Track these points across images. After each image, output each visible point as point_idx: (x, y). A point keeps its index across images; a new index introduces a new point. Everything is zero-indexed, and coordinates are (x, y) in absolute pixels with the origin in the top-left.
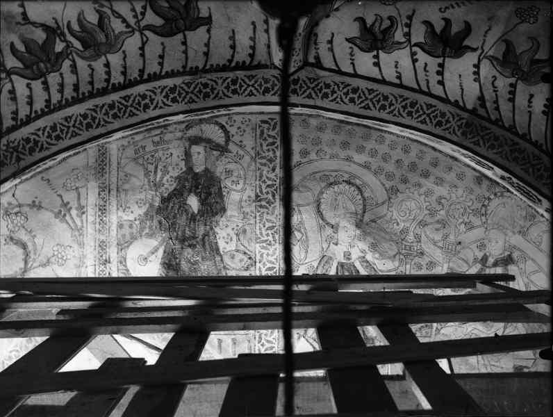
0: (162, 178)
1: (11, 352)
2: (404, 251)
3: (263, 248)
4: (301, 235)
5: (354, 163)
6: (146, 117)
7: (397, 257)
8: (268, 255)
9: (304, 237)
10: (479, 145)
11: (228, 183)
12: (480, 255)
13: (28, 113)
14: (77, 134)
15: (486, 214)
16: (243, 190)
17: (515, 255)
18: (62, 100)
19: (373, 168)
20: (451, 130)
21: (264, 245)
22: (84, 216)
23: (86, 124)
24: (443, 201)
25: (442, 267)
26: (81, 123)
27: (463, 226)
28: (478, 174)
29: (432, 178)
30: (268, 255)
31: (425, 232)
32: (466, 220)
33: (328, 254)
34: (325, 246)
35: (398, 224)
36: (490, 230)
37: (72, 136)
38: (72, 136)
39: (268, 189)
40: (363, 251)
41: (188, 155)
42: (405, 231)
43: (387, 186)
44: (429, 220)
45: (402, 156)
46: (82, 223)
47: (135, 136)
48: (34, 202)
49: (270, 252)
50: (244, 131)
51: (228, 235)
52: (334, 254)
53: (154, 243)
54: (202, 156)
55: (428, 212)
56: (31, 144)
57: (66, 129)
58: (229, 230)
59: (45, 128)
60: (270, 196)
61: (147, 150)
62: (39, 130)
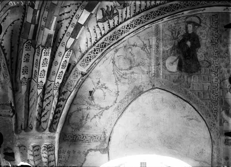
0: (178, 35)
1: (126, 96)
3: (214, 59)
4: (227, 54)
6: (178, 11)
8: (216, 62)
11: (201, 37)
13: (139, 11)
14: (154, 18)
16: (206, 39)
18: (140, 11)
21: (215, 58)
22: (151, 49)
23: (138, 23)
26: (156, 14)
30: (216, 62)
37: (153, 18)
38: (153, 18)
39: (216, 38)
41: (187, 28)
46: (150, 51)
47: (168, 21)
48: (134, 44)
49: (217, 61)
50: (206, 19)
51: (201, 55)
53: (175, 58)
54: (191, 28)
56: (139, 21)
57: (132, 25)
58: (202, 53)
59: (144, 16)
60: (216, 41)
61: (172, 26)
62: (142, 16)
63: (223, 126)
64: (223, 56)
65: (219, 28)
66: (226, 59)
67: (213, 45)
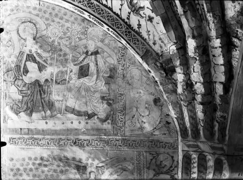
2: (53, 49)
4: (11, 43)
5: (32, 14)
7: (51, 51)
9: (13, 44)
12: (85, 51)
15: (87, 34)
17: (100, 50)
19: (40, 16)
24: (69, 29)
25: (70, 55)
27: (78, 38)
28: (83, 18)
29: (64, 20)
31: (62, 41)
32: (79, 36)
33: (23, 50)
34: (21, 47)
35: (51, 38)
36: (88, 40)
40: (37, 49)
42: (53, 41)
43: (46, 23)
44: (63, 36)
45: (52, 11)
52: (25, 51)
55: (63, 33)
64: (7, 45)
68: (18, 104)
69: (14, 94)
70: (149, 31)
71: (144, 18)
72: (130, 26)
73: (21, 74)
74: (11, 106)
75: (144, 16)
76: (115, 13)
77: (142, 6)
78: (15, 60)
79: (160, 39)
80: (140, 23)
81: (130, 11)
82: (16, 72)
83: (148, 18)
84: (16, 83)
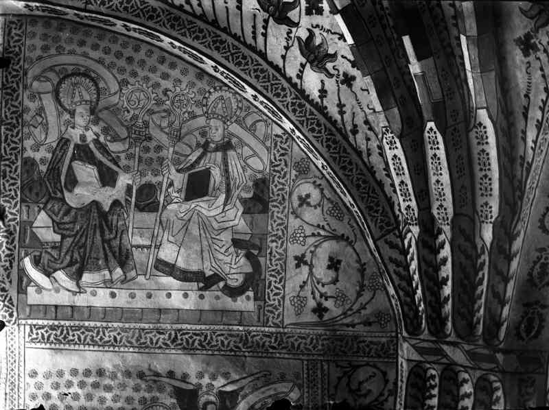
2: (133, 136)
3: (7, 129)
4: (41, 119)
5: (90, 58)
7: (128, 140)
8: (12, 136)
9: (45, 121)
10: (185, 35)
12: (202, 141)
15: (207, 105)
17: (234, 141)
19: (106, 64)
20: (161, 23)
24: (168, 93)
25: (168, 150)
27: (187, 114)
28: (199, 71)
29: (159, 74)
30: (12, 136)
31: (152, 119)
32: (189, 110)
33: (66, 136)
34: (63, 129)
35: (128, 112)
36: (210, 119)
40: (96, 134)
42: (135, 117)
43: (119, 79)
44: (156, 109)
45: (132, 54)
52: (72, 137)
55: (154, 102)
60: (15, 85)
63: (26, 294)
64: (31, 123)
65: (22, 56)
66: (38, 129)
67: (7, 94)
68: (53, 253)
69: (43, 231)
70: (344, 105)
71: (335, 78)
72: (302, 92)
73: (59, 188)
74: (35, 256)
75: (336, 72)
76: (271, 64)
77: (331, 51)
78: (49, 156)
79: (367, 122)
80: (326, 88)
81: (304, 61)
82: (50, 183)
83: (342, 77)
84: (49, 206)
